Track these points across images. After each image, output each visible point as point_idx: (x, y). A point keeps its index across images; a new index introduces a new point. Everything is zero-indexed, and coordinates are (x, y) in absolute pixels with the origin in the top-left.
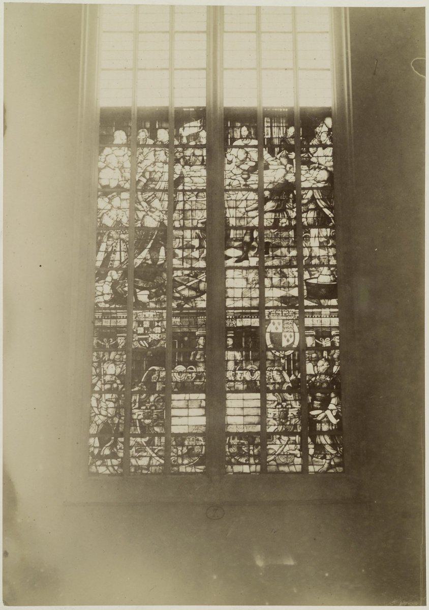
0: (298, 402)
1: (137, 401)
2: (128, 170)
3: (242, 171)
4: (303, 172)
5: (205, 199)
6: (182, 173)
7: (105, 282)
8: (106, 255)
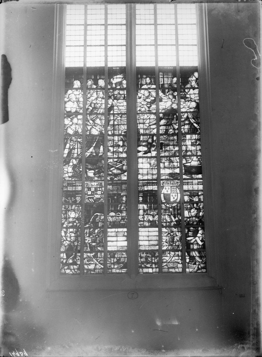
0: (180, 233)
1: (88, 232)
2: (81, 103)
3: (147, 103)
4: (182, 103)
6: (112, 104)
7: (69, 166)
8: (69, 150)
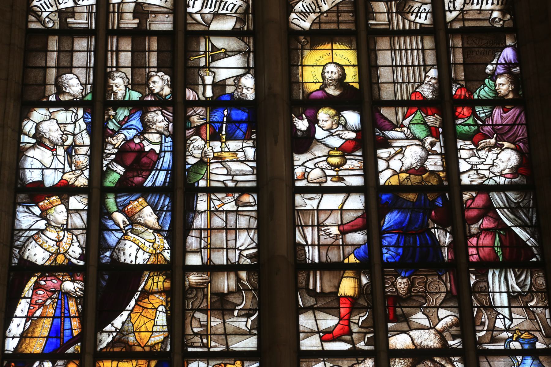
3: (327, 150)
4: (464, 154)
5: (255, 208)
6: (204, 154)
8: (28, 324)
